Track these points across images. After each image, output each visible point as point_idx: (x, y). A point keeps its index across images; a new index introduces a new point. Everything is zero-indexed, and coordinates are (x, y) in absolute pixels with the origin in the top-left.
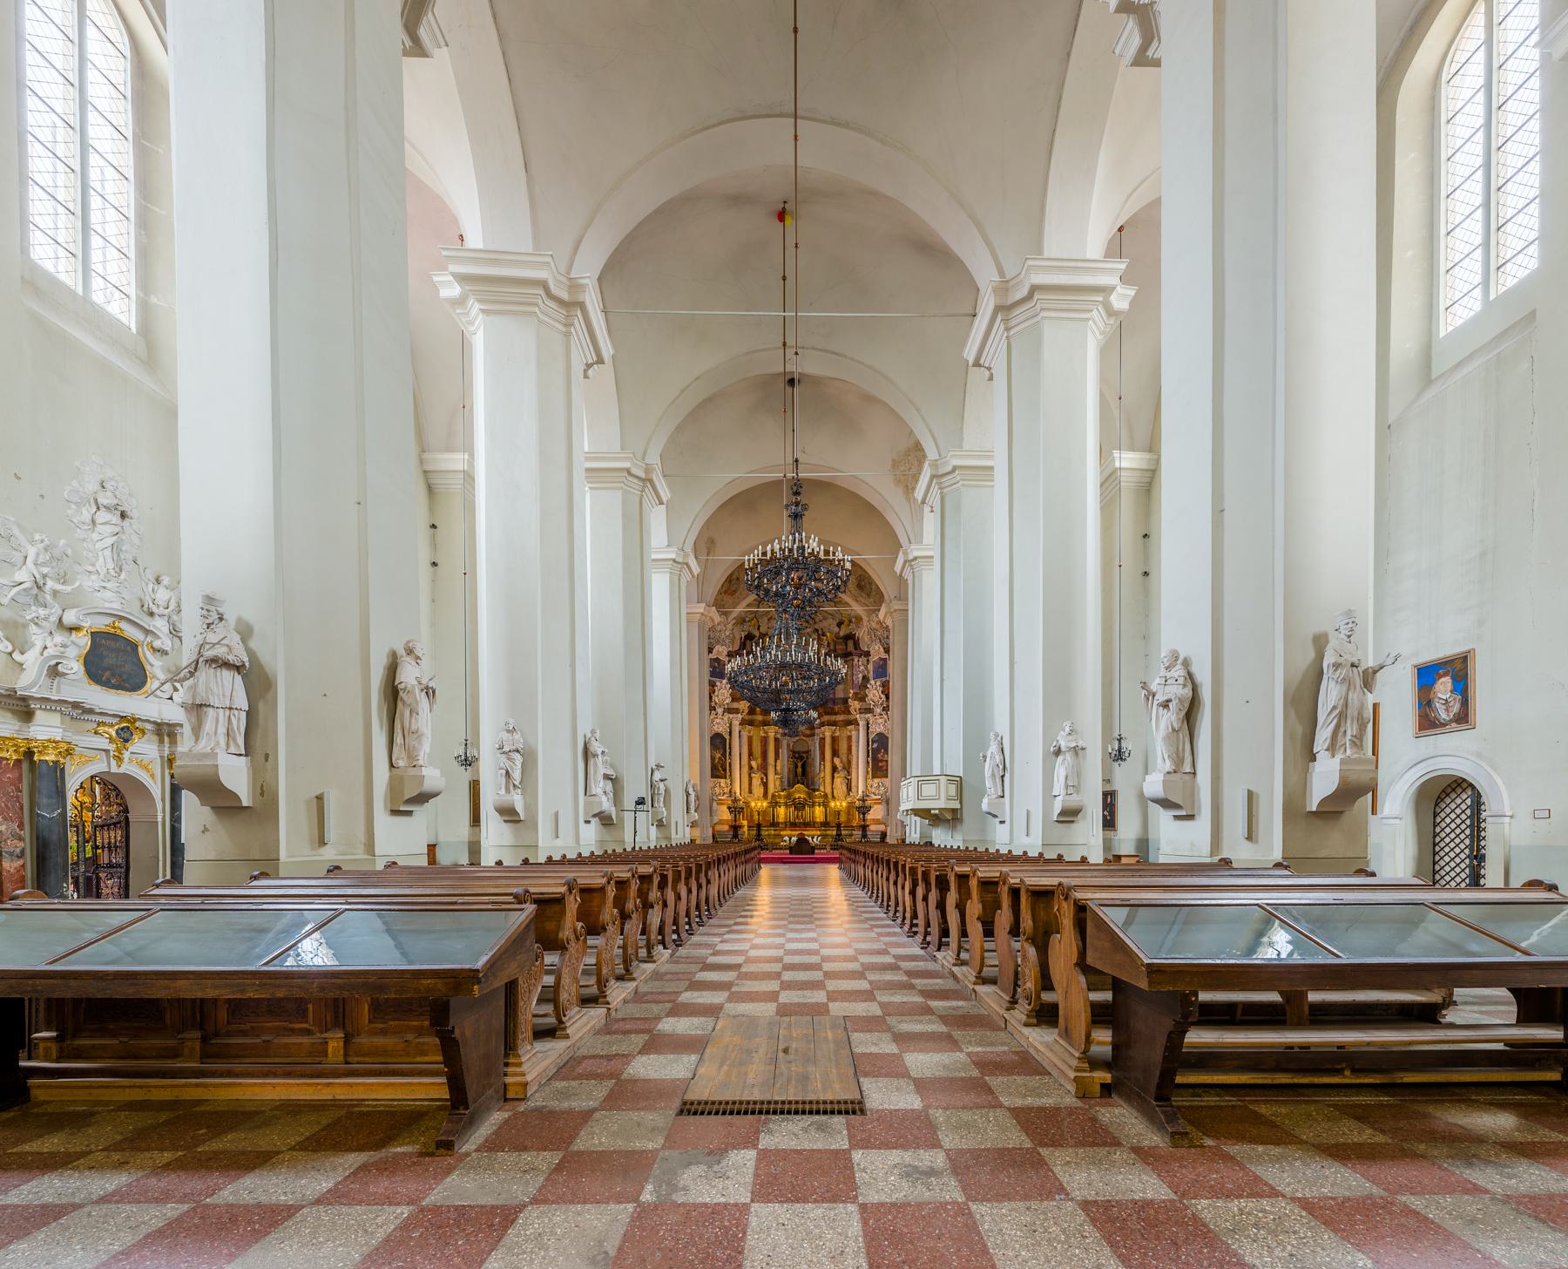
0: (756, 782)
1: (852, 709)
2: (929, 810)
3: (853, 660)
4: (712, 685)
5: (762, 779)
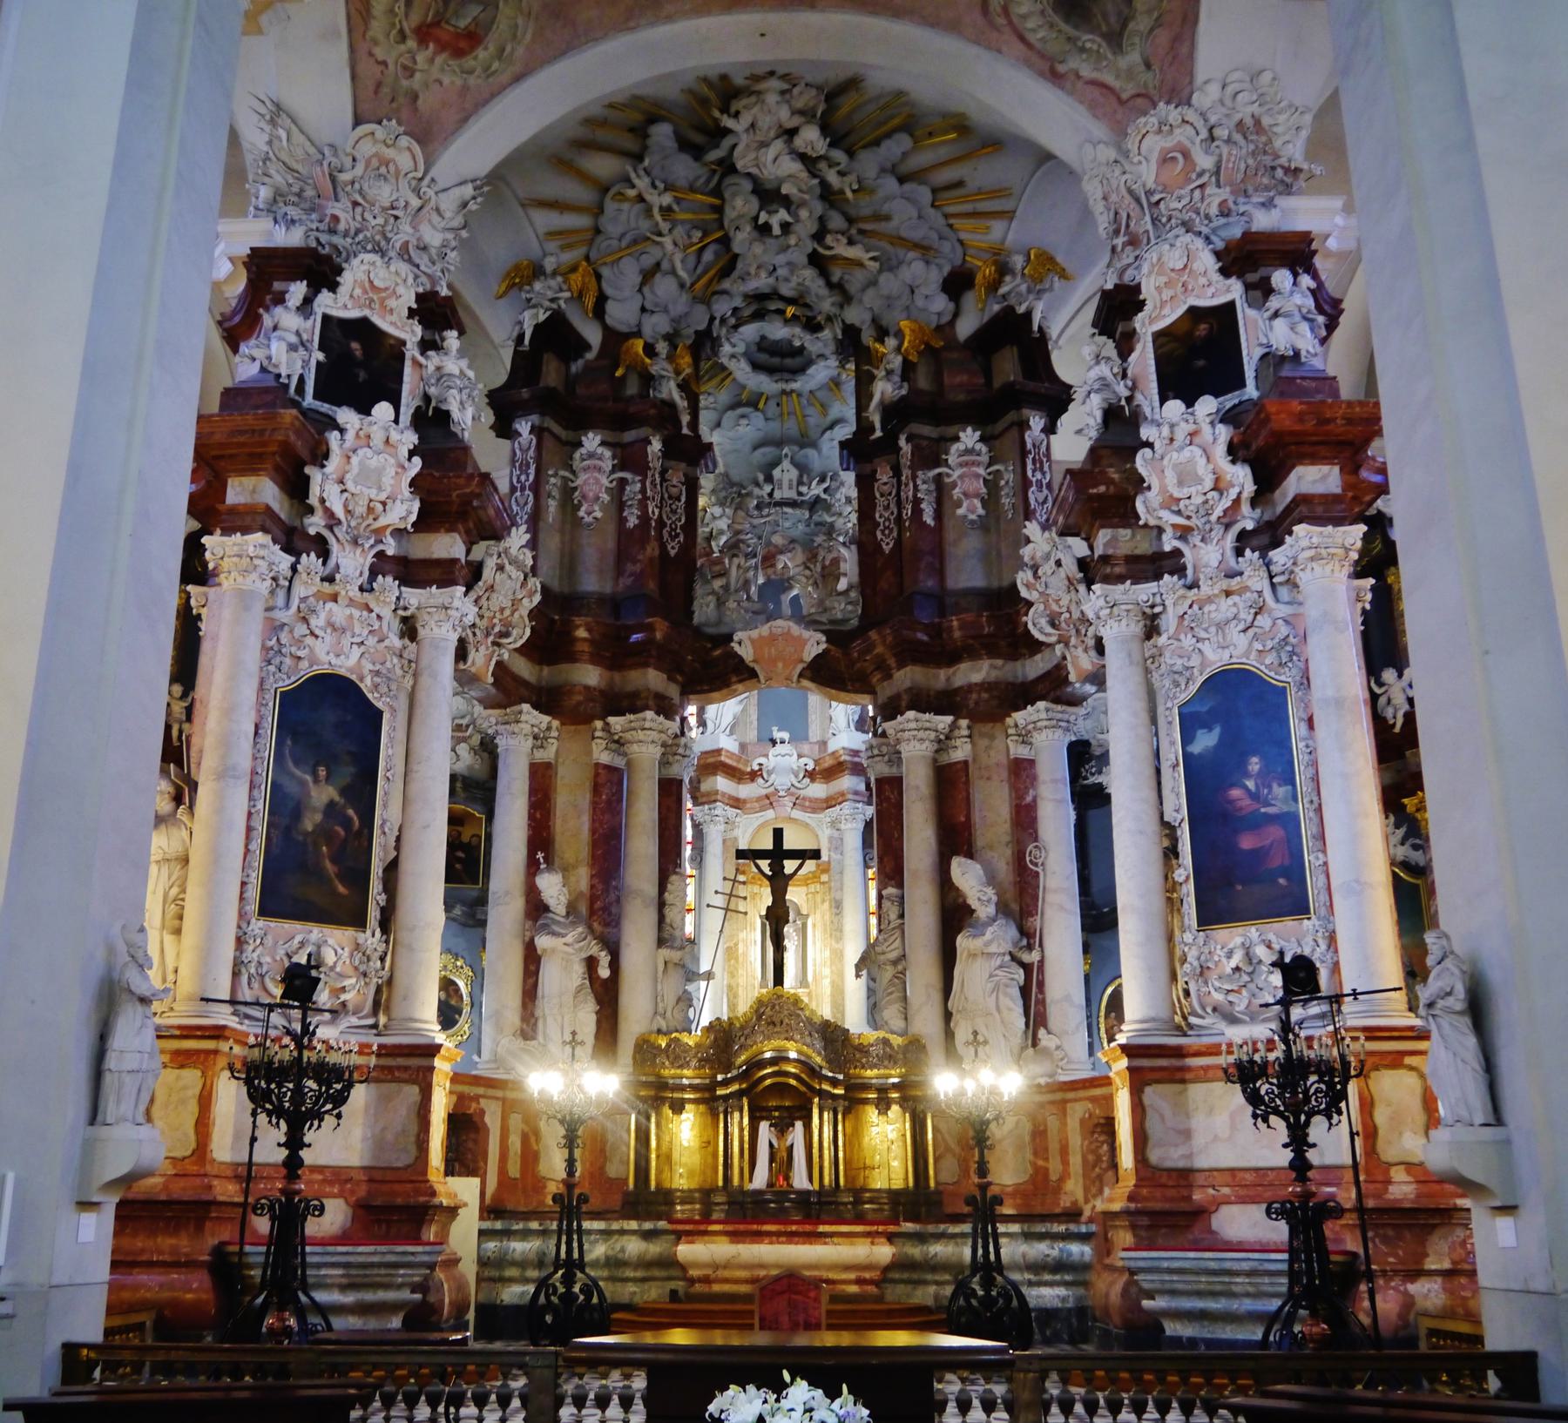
3: (1024, 425)
5: (591, 963)
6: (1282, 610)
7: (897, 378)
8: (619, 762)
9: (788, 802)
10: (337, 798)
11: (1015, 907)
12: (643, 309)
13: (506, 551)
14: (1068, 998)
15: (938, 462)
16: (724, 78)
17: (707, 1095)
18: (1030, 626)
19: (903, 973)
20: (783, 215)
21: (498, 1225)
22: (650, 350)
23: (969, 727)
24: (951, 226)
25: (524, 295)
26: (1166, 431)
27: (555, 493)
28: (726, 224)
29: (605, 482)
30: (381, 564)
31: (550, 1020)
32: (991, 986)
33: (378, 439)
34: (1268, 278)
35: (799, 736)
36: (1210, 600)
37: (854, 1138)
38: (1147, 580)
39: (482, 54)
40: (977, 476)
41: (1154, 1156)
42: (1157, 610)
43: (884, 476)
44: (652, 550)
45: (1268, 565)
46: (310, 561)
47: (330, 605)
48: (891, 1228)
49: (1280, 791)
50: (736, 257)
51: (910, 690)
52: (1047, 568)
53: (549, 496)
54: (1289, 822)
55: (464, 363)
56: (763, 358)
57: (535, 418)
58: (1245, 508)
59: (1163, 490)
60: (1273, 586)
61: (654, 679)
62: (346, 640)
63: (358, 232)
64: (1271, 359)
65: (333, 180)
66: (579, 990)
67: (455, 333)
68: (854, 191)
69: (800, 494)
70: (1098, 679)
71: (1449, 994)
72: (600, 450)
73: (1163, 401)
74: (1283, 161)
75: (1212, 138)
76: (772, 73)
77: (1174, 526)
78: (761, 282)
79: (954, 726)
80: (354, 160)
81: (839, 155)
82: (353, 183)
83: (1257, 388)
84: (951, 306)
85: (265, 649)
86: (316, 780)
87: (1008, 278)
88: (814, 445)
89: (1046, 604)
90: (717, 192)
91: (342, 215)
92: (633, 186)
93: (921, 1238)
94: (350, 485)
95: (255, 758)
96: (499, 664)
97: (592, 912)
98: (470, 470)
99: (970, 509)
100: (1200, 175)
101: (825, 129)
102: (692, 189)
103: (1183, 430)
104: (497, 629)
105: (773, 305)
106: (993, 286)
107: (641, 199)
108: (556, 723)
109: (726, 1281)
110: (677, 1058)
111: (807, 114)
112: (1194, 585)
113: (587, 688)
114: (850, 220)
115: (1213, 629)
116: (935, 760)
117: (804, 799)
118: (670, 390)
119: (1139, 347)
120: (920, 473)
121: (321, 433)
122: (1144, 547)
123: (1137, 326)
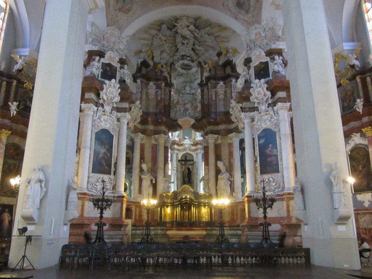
0: (146, 183)
3: (231, 81)
5: (152, 180)
6: (276, 118)
7: (208, 72)
8: (157, 143)
9: (188, 150)
10: (106, 151)
11: (229, 170)
12: (161, 59)
13: (136, 105)
14: (238, 187)
15: (215, 88)
16: (175, 16)
17: (173, 204)
18: (232, 119)
19: (209, 182)
20: (187, 41)
21: (135, 228)
22: (162, 66)
23: (221, 137)
24: (218, 44)
25: (139, 56)
26: (255, 85)
27: (145, 93)
28: (176, 42)
29: (154, 91)
30: (113, 108)
31: (144, 191)
32: (224, 184)
33: (112, 85)
34: (274, 57)
35: (190, 138)
36: (263, 116)
37: (199, 212)
38: (252, 112)
39: (131, 13)
40: (223, 90)
41: (252, 215)
42: (254, 117)
43: (206, 90)
44: (163, 104)
45: (273, 109)
46: (100, 108)
47: (104, 116)
48: (206, 228)
49: (275, 150)
50: (178, 49)
51: (210, 130)
52: (235, 108)
53: (144, 94)
54: (276, 156)
55: (128, 71)
56: (184, 67)
57: (141, 79)
58: (270, 99)
59: (255, 95)
60: (274, 113)
61: (163, 128)
62: (107, 123)
64: (275, 72)
65: (103, 37)
66: (149, 186)
67: (126, 66)
68: (200, 37)
69: (190, 92)
70: (244, 128)
71: (298, 188)
72: (153, 85)
73: (255, 79)
74: (277, 35)
75: (265, 30)
76: (184, 16)
77: (257, 102)
78: (183, 53)
79: (218, 137)
80: (107, 33)
81: (197, 31)
82: (107, 38)
83: (272, 77)
84: (218, 58)
85: (92, 124)
86: (102, 148)
87: (228, 53)
88: (193, 83)
89: (235, 115)
90: (174, 37)
91: (105, 44)
92: (159, 36)
93: (211, 230)
94: (107, 94)
95: (91, 144)
96: (135, 126)
97: (152, 171)
98: (129, 91)
99: (222, 97)
101: (195, 26)
102: (170, 36)
103: (258, 85)
104: (134, 119)
105: (185, 57)
106: (226, 55)
107: (160, 38)
108: (145, 136)
109: (176, 238)
110: (167, 197)
111: (191, 23)
112: (260, 113)
113: (151, 129)
114: (199, 42)
115: (264, 121)
116: (215, 143)
117: (191, 149)
118: (166, 74)
119: (251, 69)
120: (212, 90)
121: (102, 85)
122: (251, 106)
123: (251, 65)
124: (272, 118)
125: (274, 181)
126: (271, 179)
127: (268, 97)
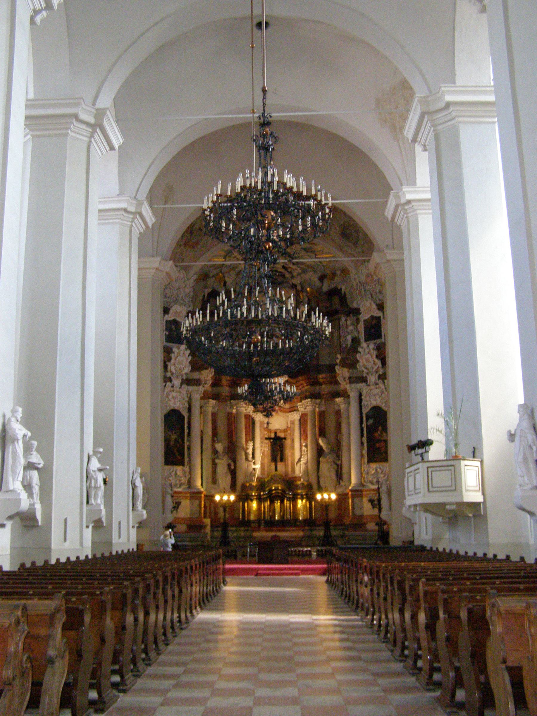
1: (339, 379)
2: (443, 505)
3: (340, 319)
4: (168, 352)
5: (229, 465)
11: (335, 449)
37: (295, 506)
39: (199, 247)
46: (168, 384)
47: (173, 393)
49: (384, 434)
54: (386, 441)
58: (380, 369)
60: (386, 388)
63: (172, 296)
66: (226, 473)
100: (375, 281)
103: (367, 351)
106: (333, 279)
112: (369, 385)
122: (360, 375)
124: (383, 393)
125: (382, 472)
126: (379, 470)
127: (379, 367)
